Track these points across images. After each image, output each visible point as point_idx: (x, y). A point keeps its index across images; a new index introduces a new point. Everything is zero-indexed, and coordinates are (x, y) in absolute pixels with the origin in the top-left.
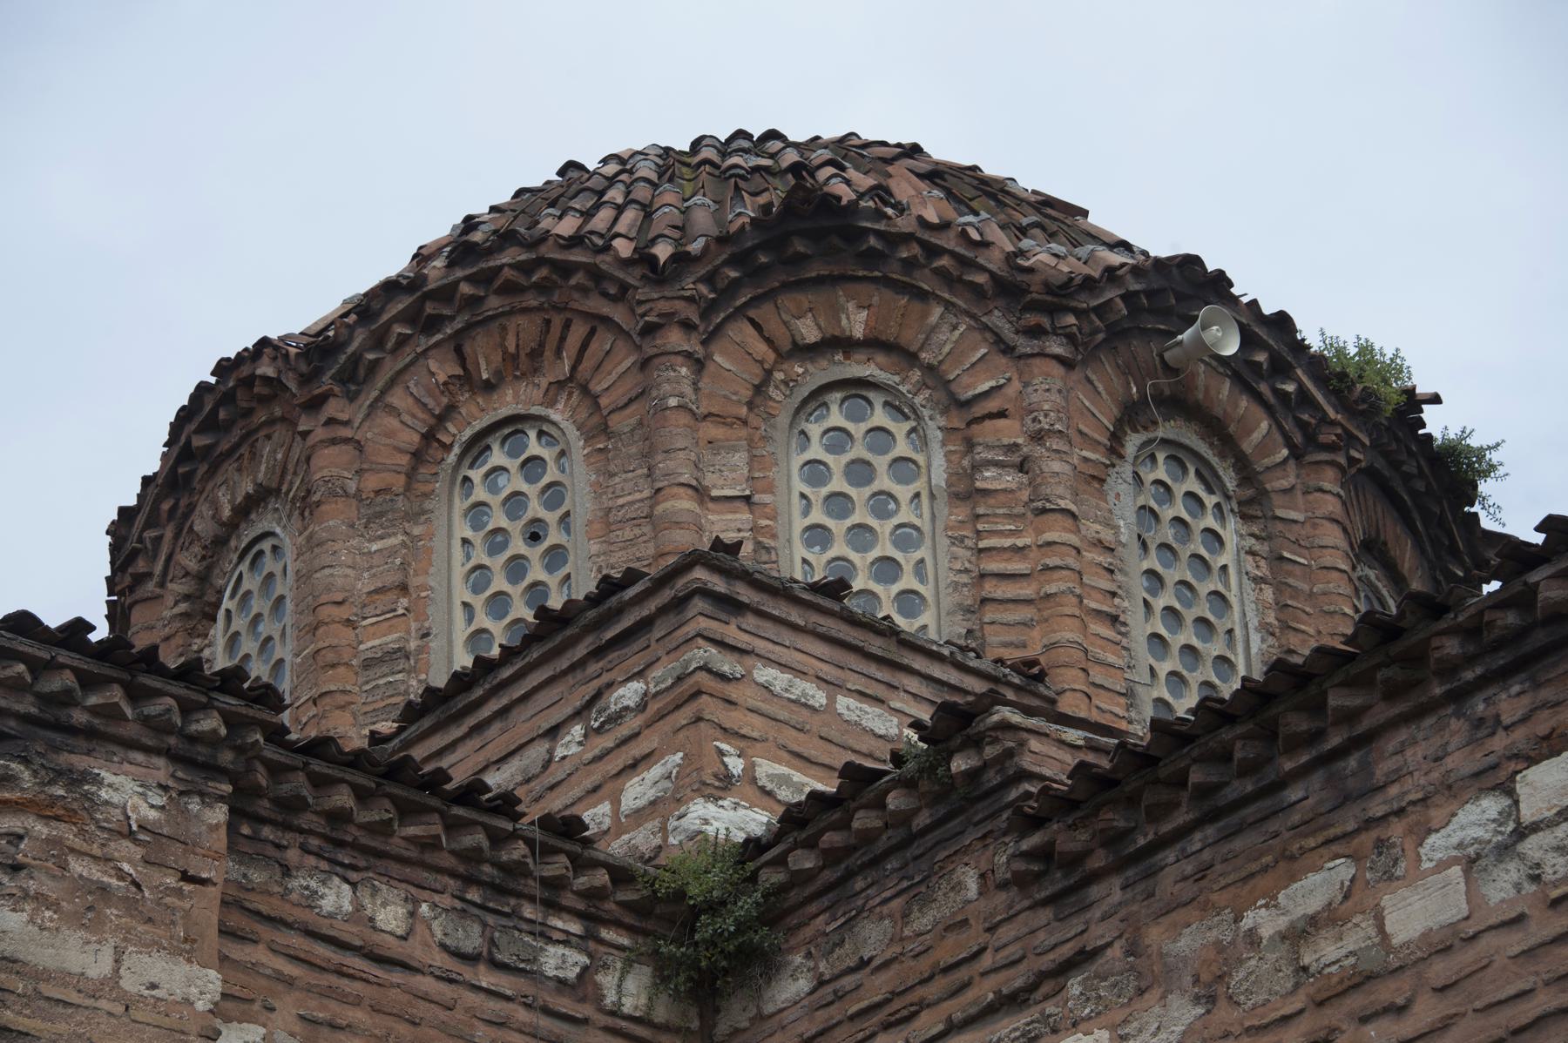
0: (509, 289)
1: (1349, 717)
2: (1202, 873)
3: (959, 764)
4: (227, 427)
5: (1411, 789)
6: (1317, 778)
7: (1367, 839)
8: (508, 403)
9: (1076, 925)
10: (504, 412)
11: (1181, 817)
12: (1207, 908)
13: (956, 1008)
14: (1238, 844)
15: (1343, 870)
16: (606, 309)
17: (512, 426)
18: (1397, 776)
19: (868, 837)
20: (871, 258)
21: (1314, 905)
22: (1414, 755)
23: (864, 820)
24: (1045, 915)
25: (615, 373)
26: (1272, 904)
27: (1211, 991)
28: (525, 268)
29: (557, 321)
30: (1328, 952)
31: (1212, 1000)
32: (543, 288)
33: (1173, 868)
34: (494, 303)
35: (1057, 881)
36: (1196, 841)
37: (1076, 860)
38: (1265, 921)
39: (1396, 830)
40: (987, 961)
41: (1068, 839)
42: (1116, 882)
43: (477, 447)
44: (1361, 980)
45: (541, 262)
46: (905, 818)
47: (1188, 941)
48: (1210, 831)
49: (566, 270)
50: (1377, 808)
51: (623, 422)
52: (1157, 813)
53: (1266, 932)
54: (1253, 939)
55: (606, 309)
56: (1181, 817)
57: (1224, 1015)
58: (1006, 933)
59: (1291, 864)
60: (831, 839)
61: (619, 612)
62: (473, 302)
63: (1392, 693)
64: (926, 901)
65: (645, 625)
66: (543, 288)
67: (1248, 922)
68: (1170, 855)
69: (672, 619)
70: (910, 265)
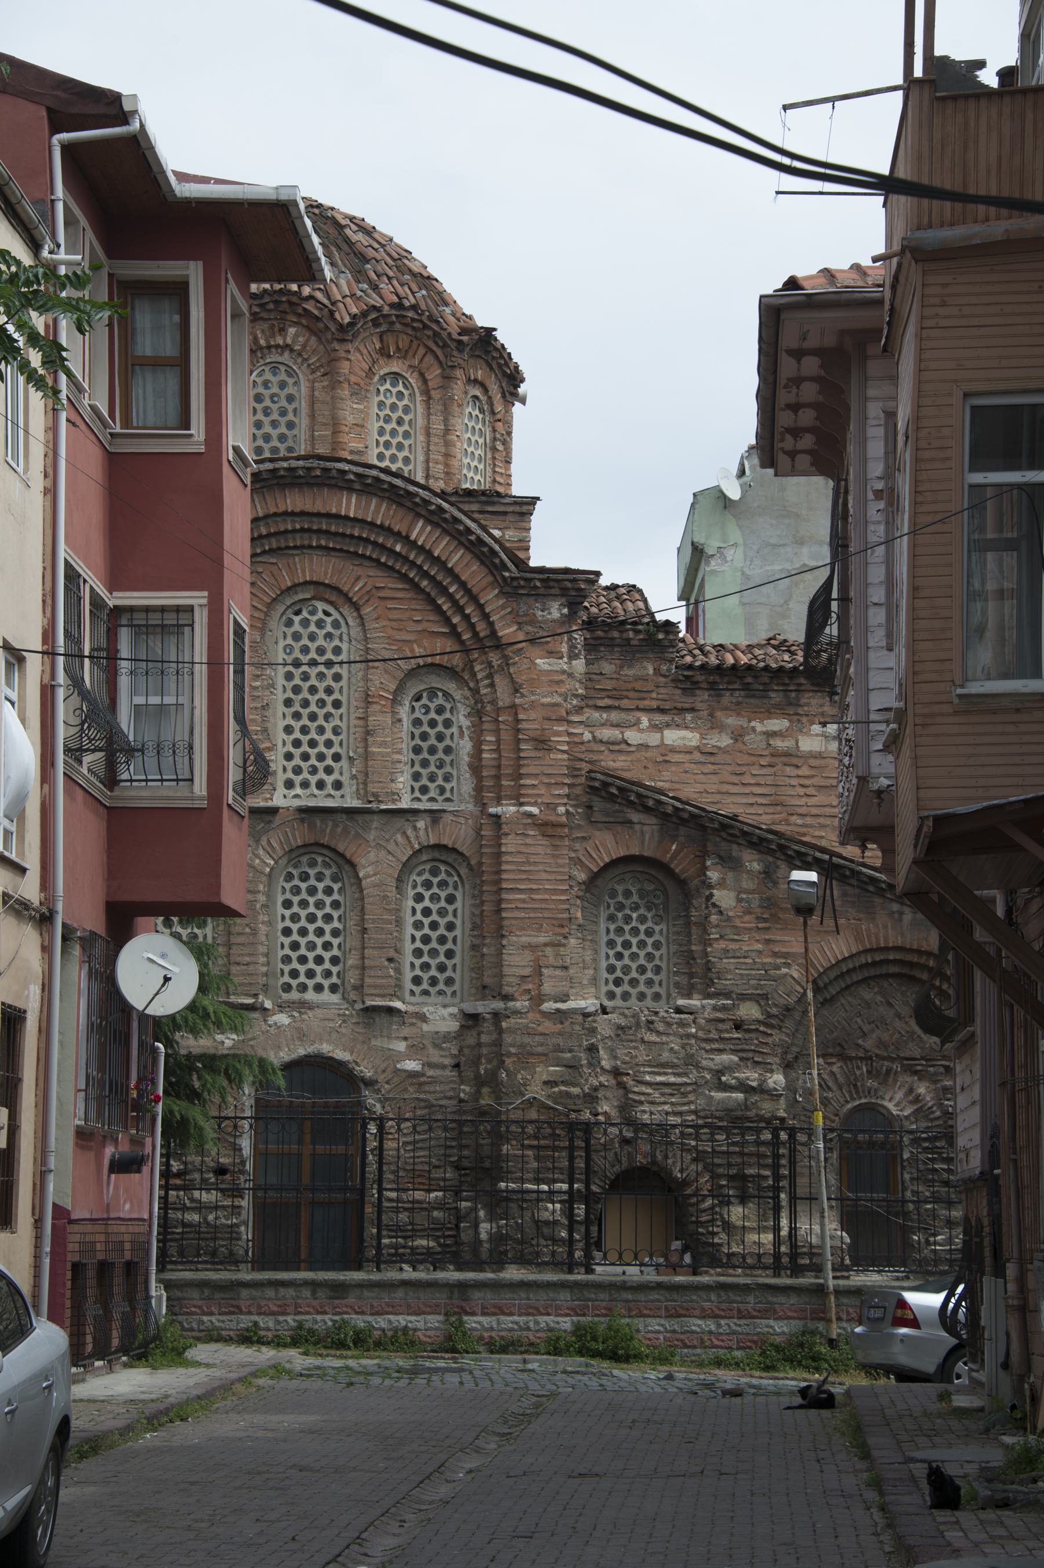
0: (406, 325)
1: (800, 685)
2: (738, 703)
3: (661, 636)
4: (269, 311)
5: (813, 710)
6: (781, 694)
7: (796, 718)
8: (396, 366)
9: (691, 700)
10: (395, 369)
11: (736, 686)
12: (738, 714)
13: (642, 704)
14: (752, 701)
15: (786, 723)
16: (435, 348)
17: (396, 377)
18: (807, 704)
19: (613, 639)
20: (487, 352)
21: (776, 728)
22: (814, 702)
23: (615, 634)
24: (679, 692)
25: (434, 374)
26: (762, 722)
27: (738, 736)
28: (413, 320)
29: (415, 343)
30: (779, 743)
31: (736, 740)
32: (414, 328)
33: (727, 699)
34: (398, 326)
35: (688, 685)
36: (737, 694)
37: (698, 682)
38: (759, 727)
39: (804, 719)
40: (654, 695)
41: (700, 678)
42: (707, 693)
43: (383, 379)
44: (787, 754)
45: (421, 321)
46: (628, 640)
47: (731, 721)
48: (743, 693)
49: (425, 327)
50: (800, 711)
51: (436, 394)
52: (729, 683)
53: (758, 729)
54: (754, 729)
55: (435, 348)
56: (736, 686)
57: (739, 745)
58: (662, 690)
59: (769, 714)
60: (600, 633)
61: (493, 503)
62: (392, 323)
63: (813, 685)
64: (630, 666)
65: (505, 513)
66: (414, 328)
67: (753, 724)
68: (728, 694)
69: (518, 518)
70: (493, 358)
